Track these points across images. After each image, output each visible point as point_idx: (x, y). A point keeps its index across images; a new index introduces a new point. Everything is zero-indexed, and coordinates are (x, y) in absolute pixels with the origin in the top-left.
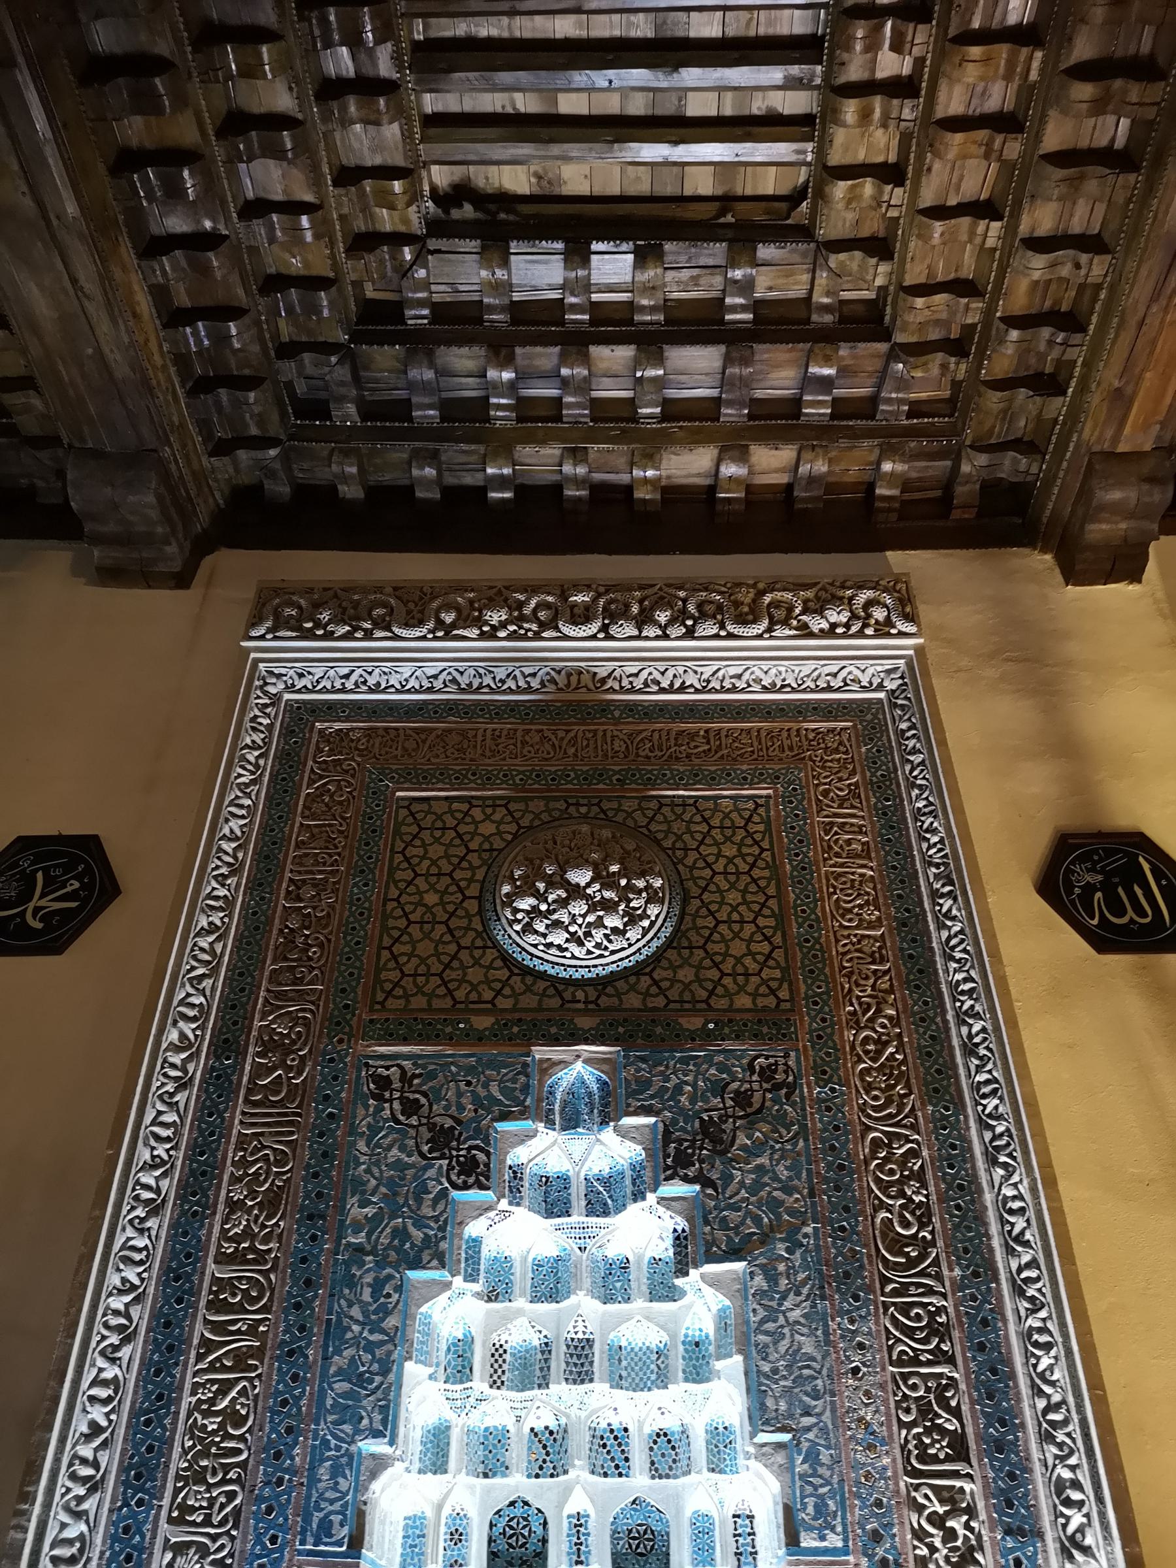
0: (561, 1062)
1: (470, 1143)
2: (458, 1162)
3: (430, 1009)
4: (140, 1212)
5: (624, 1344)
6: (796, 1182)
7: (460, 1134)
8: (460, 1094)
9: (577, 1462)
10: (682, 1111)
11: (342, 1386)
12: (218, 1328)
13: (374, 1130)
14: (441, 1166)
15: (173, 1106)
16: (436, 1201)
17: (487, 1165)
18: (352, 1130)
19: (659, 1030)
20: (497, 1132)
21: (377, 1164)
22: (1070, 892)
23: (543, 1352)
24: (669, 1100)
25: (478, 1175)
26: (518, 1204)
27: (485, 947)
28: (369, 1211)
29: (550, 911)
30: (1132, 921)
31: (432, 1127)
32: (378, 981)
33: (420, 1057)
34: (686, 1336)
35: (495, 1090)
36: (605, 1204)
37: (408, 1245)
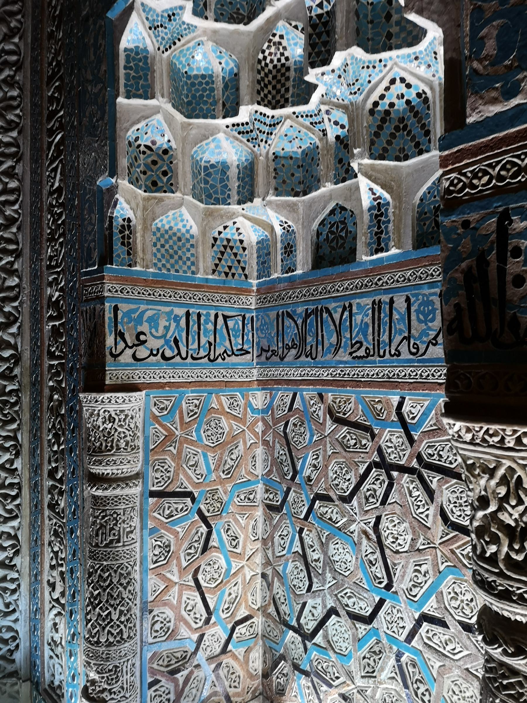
9: (356, 151)
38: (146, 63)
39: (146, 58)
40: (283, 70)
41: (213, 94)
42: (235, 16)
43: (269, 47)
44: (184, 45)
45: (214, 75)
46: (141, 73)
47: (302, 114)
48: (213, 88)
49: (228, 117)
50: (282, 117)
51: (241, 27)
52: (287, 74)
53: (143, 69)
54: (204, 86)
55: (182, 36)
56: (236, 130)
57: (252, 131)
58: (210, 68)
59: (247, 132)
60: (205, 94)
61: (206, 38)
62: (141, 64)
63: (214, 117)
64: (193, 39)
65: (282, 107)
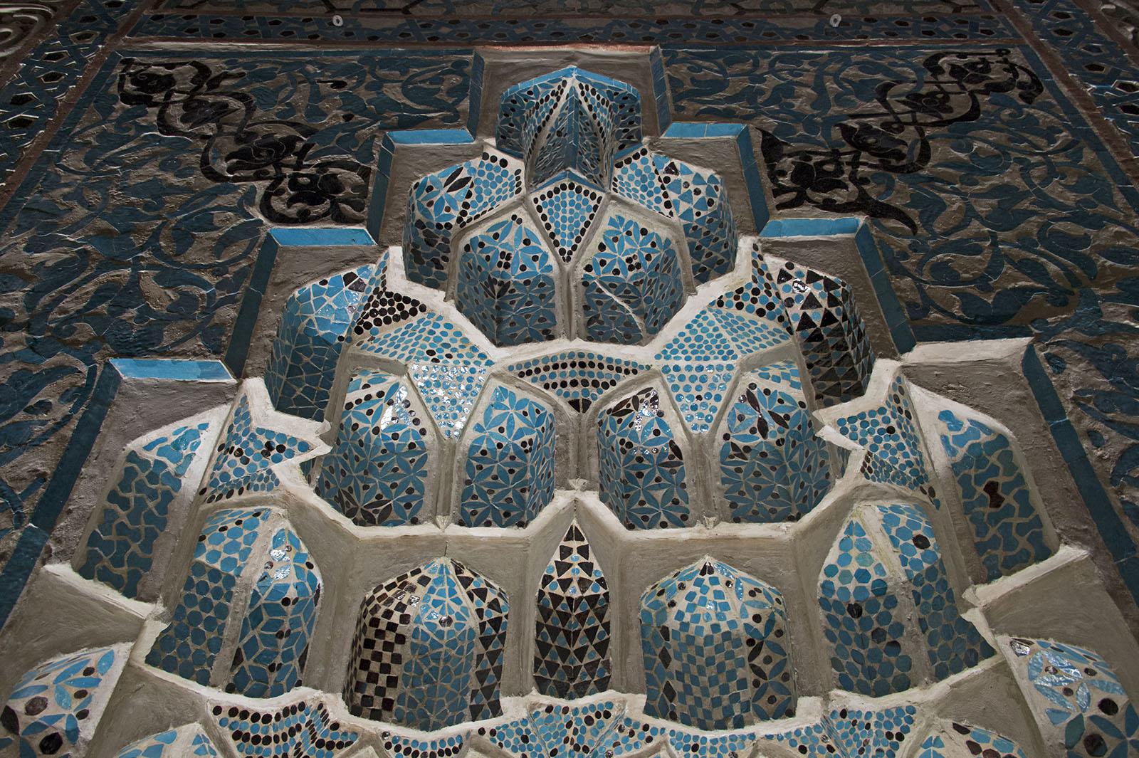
0: (534, 67)
1: (324, 158)
2: (294, 184)
5: (672, 623)
6: (1101, 209)
7: (307, 147)
8: (316, 96)
10: (798, 117)
14: (253, 190)
16: (226, 242)
17: (363, 190)
19: (730, 30)
20: (391, 147)
21: (102, 186)
23: (486, 641)
24: (766, 103)
25: (334, 203)
26: (433, 285)
33: (241, 54)
34: (827, 587)
36: (630, 324)
37: (133, 312)
38: (163, 508)
39: (168, 497)
40: (390, 637)
41: (220, 622)
42: (345, 499)
43: (389, 588)
44: (240, 504)
45: (238, 581)
46: (143, 526)
47: (401, 743)
48: (226, 608)
49: (240, 692)
50: (355, 734)
51: (347, 523)
52: (398, 649)
53: (150, 517)
54: (209, 595)
55: (248, 488)
56: (231, 728)
57: (267, 740)
58: (240, 563)
59: (256, 740)
60: (205, 615)
61: (282, 511)
62: (151, 504)
63: (204, 680)
64: (252, 503)
65: (375, 716)
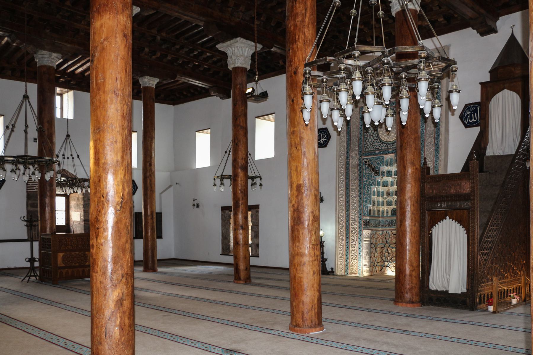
3: (371, 151)
4: (341, 182)
8: (375, 163)
11: (365, 199)
12: (352, 194)
13: (365, 169)
15: (343, 168)
18: (363, 169)
22: (464, 116)
27: (377, 139)
28: (366, 179)
29: (384, 134)
30: (473, 121)
31: (372, 168)
32: (364, 147)
35: (379, 162)
